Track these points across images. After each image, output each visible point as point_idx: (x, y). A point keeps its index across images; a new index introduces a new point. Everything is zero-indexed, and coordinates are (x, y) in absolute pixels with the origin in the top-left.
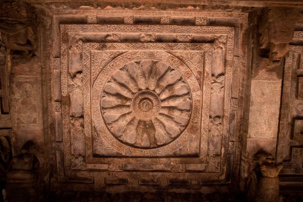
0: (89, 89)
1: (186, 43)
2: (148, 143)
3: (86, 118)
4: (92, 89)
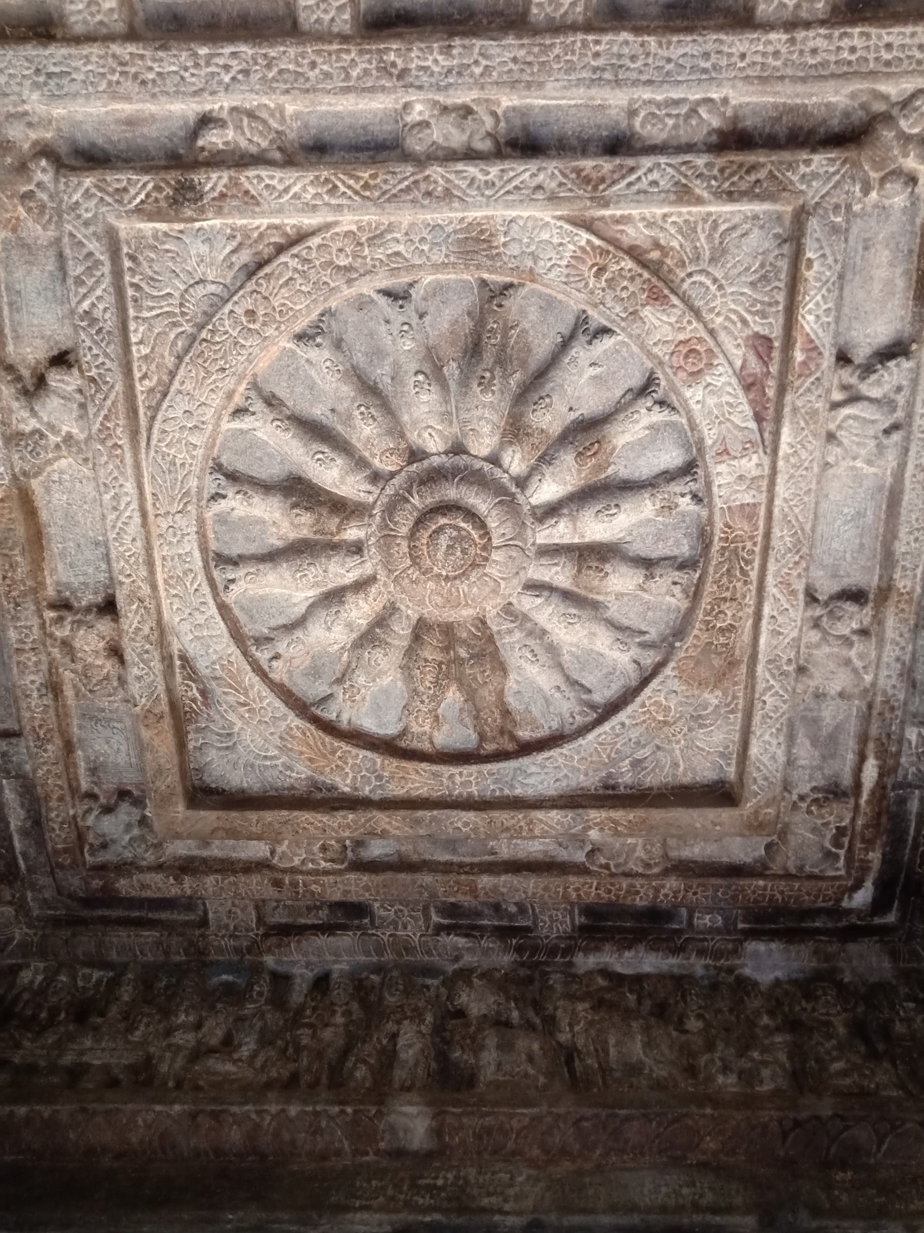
0: (128, 456)
1: (687, 158)
2: (471, 731)
3: (132, 618)
4: (147, 453)
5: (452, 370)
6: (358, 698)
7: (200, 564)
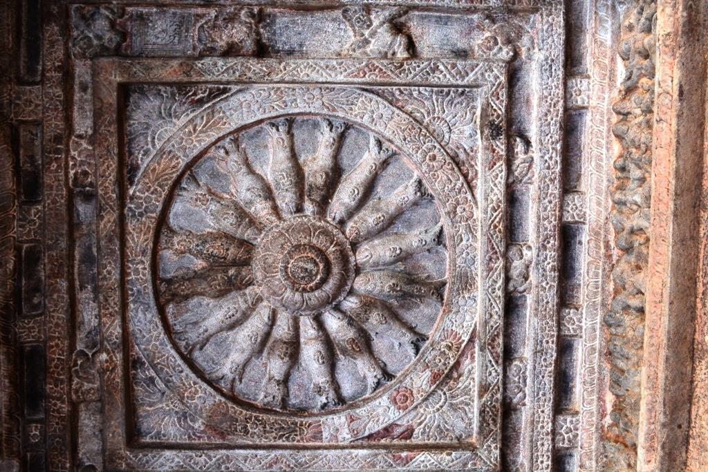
0: (360, 80)
1: (501, 389)
2: (172, 274)
4: (358, 88)
6: (199, 203)
7: (290, 112)
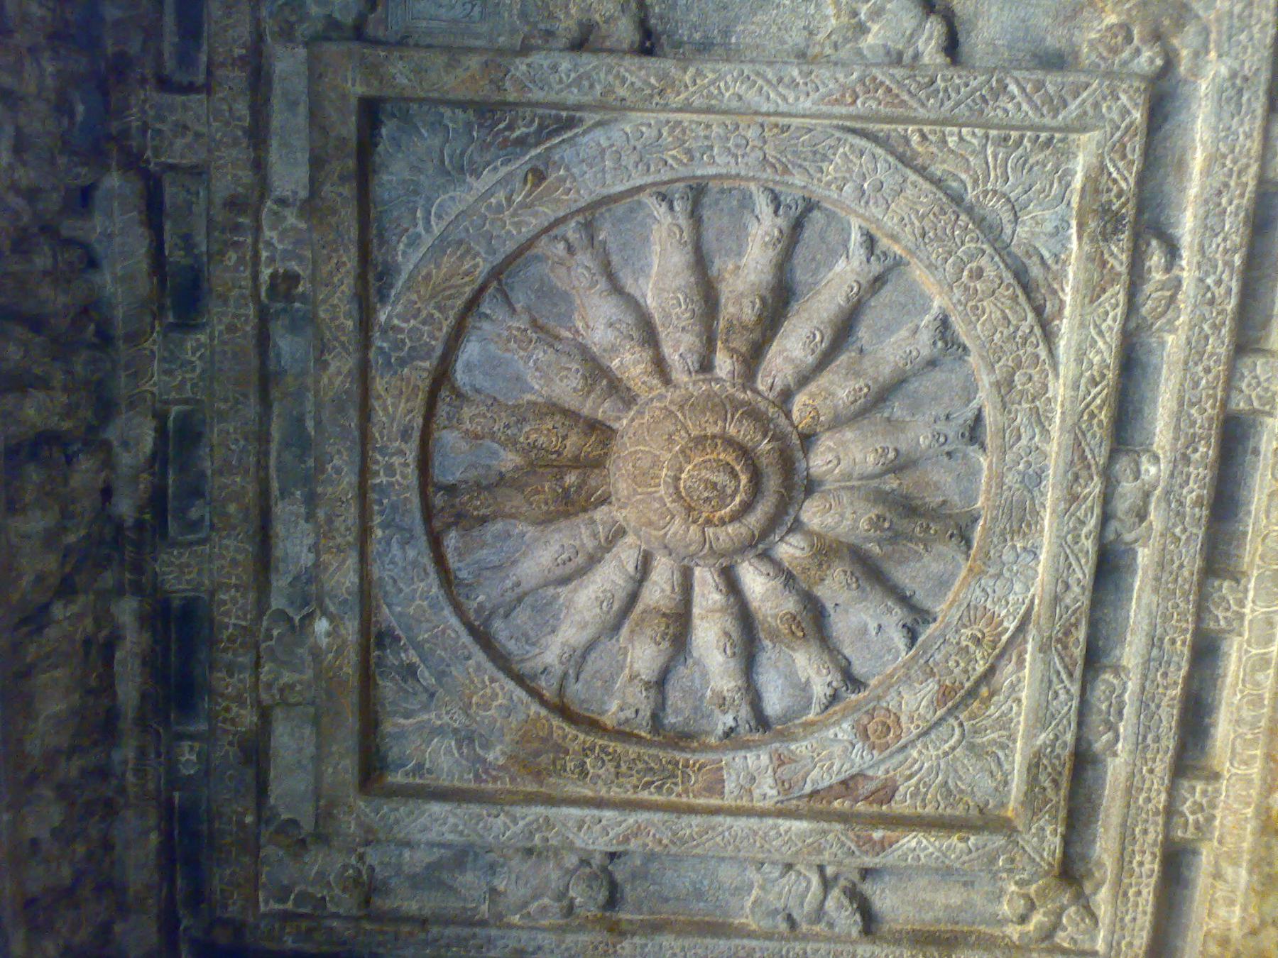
0: (844, 110)
1: (1073, 725)
2: (458, 475)
3: (637, 73)
4: (838, 127)
5: (891, 483)
6: (513, 345)
